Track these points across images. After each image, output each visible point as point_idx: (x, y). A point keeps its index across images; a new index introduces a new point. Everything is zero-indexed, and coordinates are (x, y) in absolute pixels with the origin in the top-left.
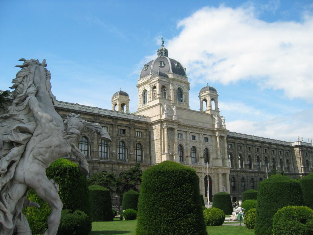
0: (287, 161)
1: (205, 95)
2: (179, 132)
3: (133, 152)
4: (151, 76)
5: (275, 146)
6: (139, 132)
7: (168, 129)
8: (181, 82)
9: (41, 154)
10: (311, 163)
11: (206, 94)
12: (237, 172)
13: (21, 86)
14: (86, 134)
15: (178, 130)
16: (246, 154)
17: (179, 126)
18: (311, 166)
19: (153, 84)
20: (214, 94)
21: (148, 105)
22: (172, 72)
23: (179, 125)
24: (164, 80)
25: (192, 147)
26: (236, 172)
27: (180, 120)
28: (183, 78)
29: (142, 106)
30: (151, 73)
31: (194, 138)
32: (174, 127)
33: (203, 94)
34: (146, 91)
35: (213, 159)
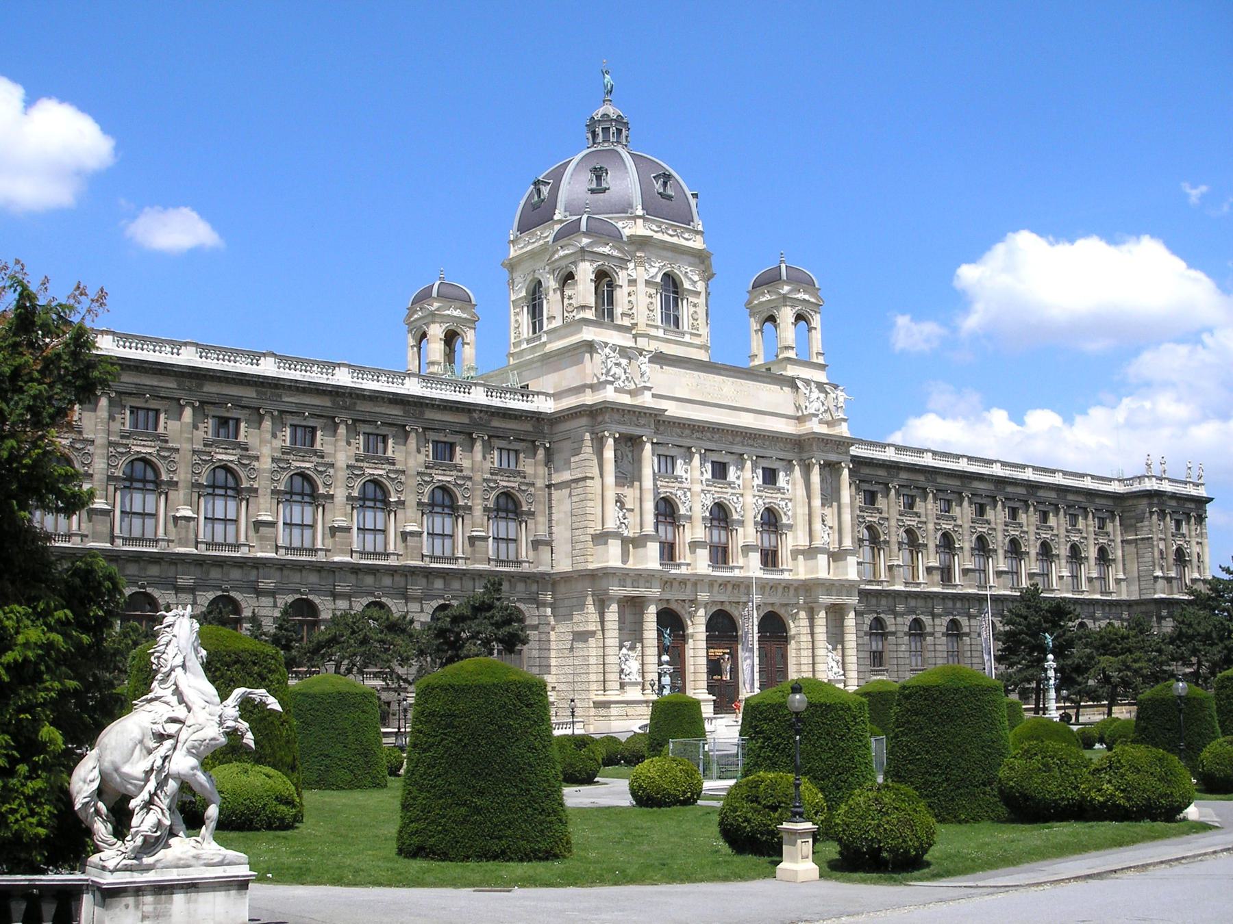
0: (1102, 552)
2: (662, 450)
3: (482, 526)
4: (557, 227)
5: (1053, 495)
6: (509, 450)
7: (615, 440)
9: (194, 747)
10: (1195, 559)
12: (894, 598)
13: (164, 656)
14: (303, 465)
16: (931, 526)
17: (662, 428)
18: (1196, 569)
19: (563, 263)
22: (640, 212)
24: (606, 250)
25: (709, 503)
26: (890, 599)
28: (686, 235)
30: (556, 217)
34: (540, 282)
35: (795, 553)
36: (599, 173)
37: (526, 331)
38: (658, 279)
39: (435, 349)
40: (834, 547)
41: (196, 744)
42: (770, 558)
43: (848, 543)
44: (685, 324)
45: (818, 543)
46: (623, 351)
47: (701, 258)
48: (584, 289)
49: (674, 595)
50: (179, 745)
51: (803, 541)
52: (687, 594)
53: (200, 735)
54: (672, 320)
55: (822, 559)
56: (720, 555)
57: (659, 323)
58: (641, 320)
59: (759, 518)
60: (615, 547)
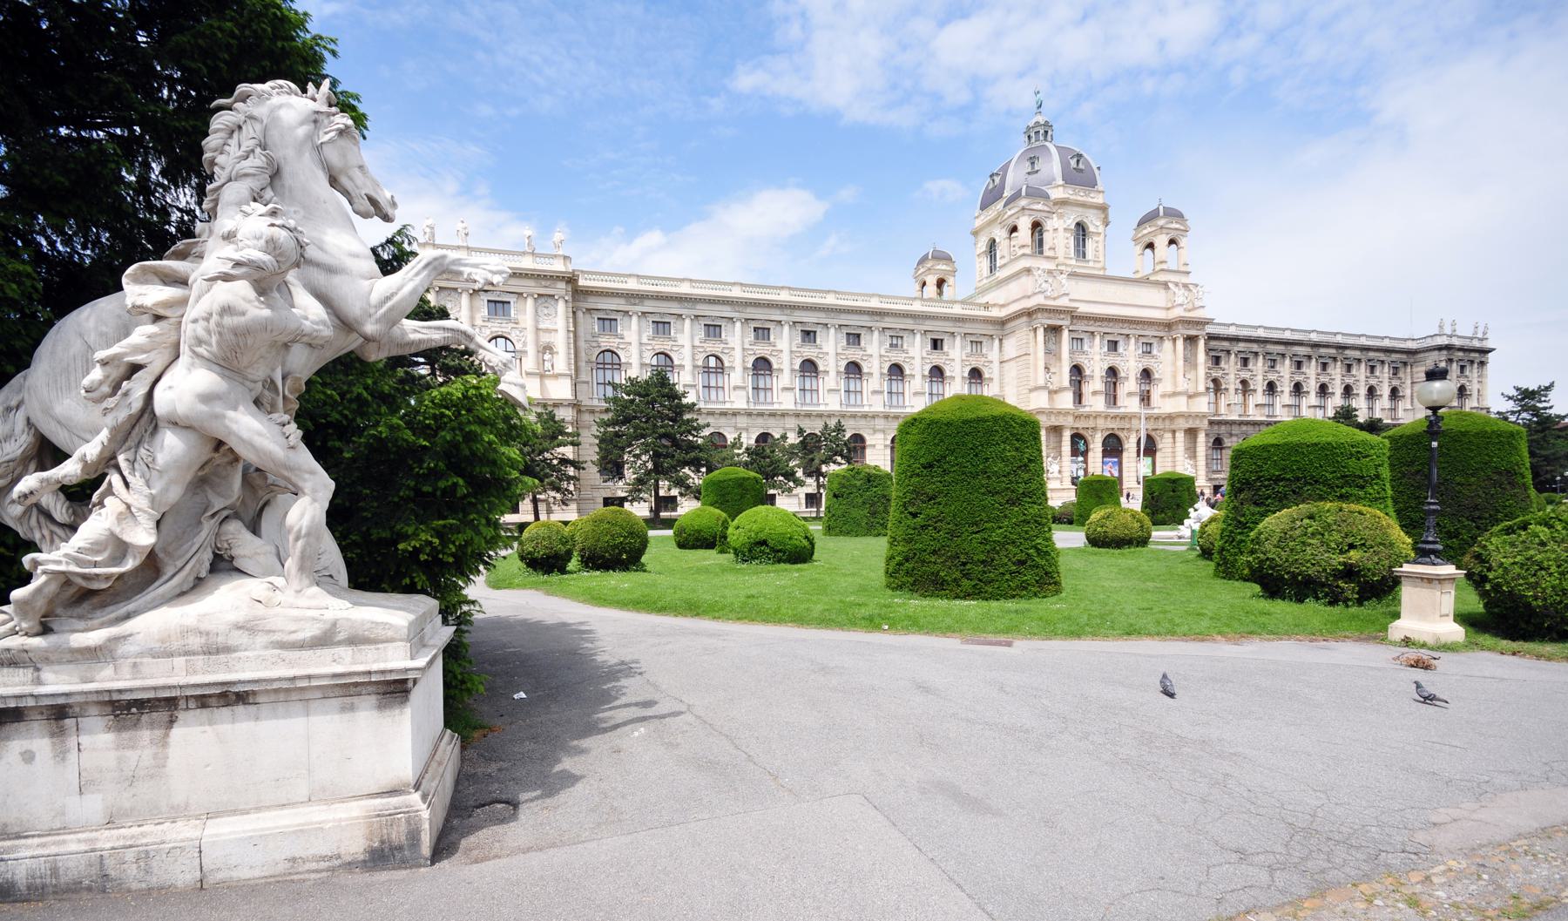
8: (1084, 205)
23: (1075, 316)
24: (1039, 207)
31: (1113, 346)
35: (1163, 396)
36: (1032, 161)
37: (986, 271)
40: (1191, 391)
42: (1145, 398)
43: (1202, 388)
44: (1089, 255)
45: (1179, 389)
46: (1050, 272)
47: (1103, 208)
49: (1080, 424)
51: (1170, 389)
52: (1091, 424)
54: (1081, 252)
55: (1184, 399)
56: (1112, 399)
58: (1060, 253)
60: (1044, 395)
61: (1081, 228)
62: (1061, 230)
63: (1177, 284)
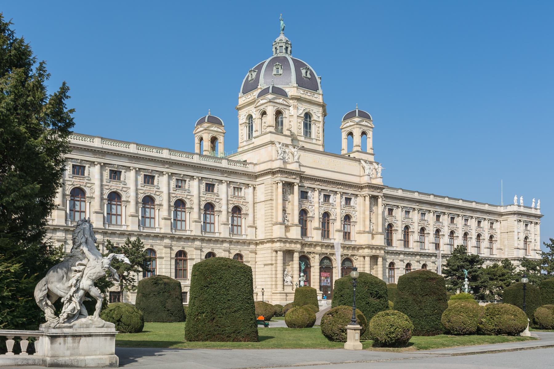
1: (350, 126)
4: (260, 90)
7: (283, 184)
11: (352, 124)
13: (77, 238)
15: (301, 186)
19: (262, 107)
20: (367, 124)
21: (253, 143)
23: (302, 177)
24: (281, 101)
27: (303, 169)
29: (245, 144)
30: (259, 87)
32: (293, 181)
33: (348, 124)
37: (245, 137)
38: (303, 115)
39: (207, 144)
41: (92, 275)
44: (313, 136)
48: (270, 118)
50: (84, 276)
53: (93, 271)
57: (303, 135)
59: (343, 219)
61: (308, 116)
62: (295, 116)
63: (365, 161)
